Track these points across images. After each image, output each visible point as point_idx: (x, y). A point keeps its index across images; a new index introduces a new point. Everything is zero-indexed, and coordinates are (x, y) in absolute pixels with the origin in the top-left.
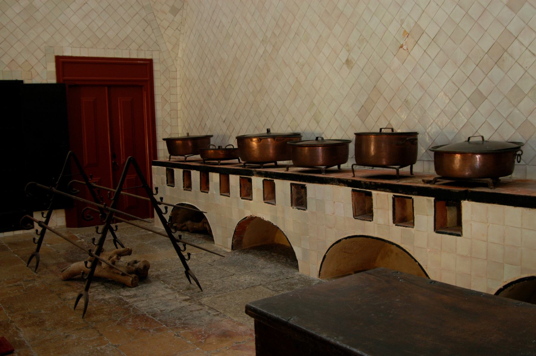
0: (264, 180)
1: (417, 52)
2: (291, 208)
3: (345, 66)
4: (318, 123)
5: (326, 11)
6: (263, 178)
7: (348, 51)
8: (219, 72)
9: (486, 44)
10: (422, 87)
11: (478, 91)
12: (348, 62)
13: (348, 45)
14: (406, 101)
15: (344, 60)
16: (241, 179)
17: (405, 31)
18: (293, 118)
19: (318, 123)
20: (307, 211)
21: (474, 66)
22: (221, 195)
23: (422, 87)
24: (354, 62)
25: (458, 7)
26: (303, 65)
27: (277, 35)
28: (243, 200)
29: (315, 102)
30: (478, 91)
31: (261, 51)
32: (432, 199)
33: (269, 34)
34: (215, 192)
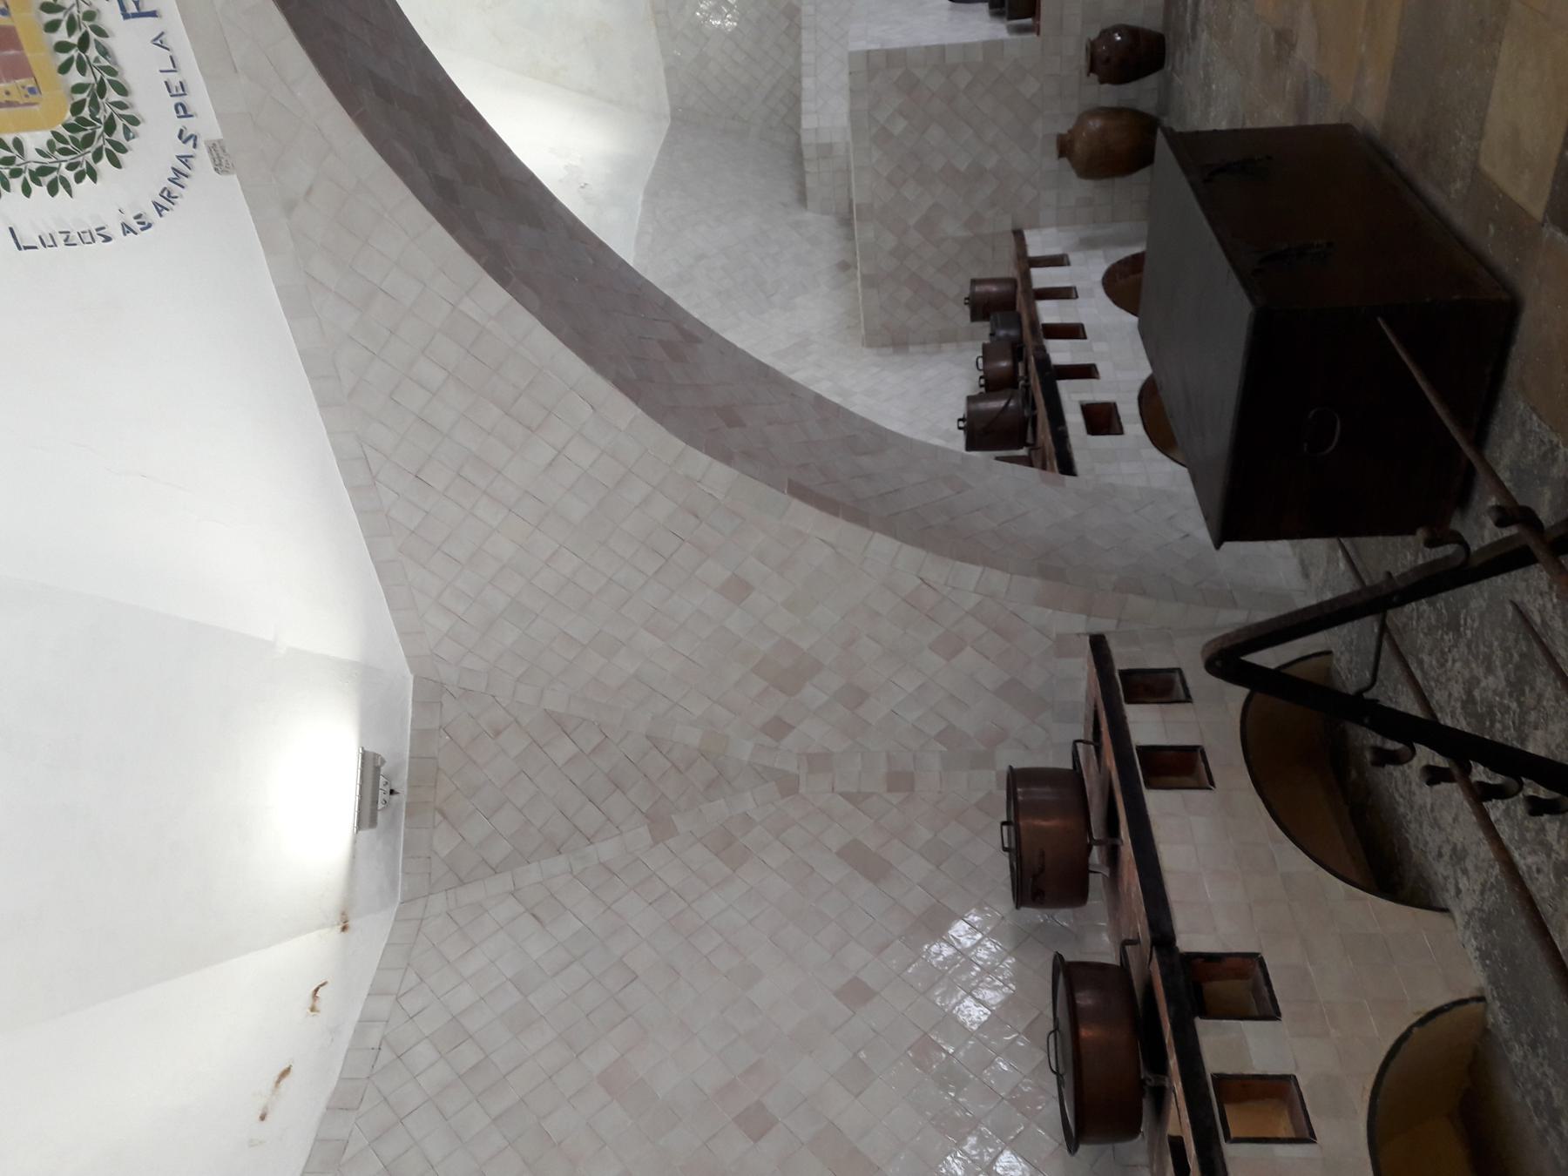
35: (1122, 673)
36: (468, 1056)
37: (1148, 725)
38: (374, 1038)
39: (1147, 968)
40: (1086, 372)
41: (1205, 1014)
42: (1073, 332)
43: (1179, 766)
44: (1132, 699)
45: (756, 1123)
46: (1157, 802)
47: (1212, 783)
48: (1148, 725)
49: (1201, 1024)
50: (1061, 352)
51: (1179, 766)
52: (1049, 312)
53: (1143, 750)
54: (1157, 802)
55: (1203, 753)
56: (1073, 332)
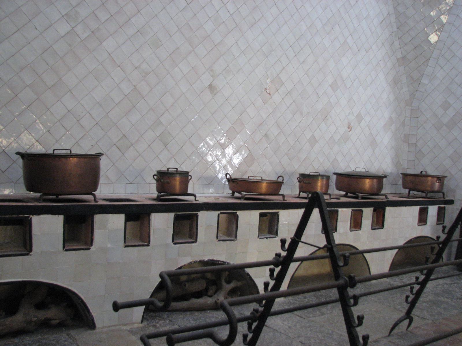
0: (221, 213)
1: (277, 98)
4: (166, 145)
7: (212, 76)
11: (313, 136)
12: (211, 87)
13: (212, 71)
14: (266, 135)
15: (207, 84)
16: (177, 219)
18: (124, 136)
19: (166, 145)
21: (312, 119)
22: (126, 246)
24: (218, 90)
25: (306, 75)
29: (162, 119)
31: (63, 28)
32: (372, 209)
37: (433, 210)
39: (382, 198)
41: (374, 210)
43: (423, 219)
44: (439, 208)
45: (334, 87)
46: (416, 209)
47: (419, 225)
48: (433, 210)
49: (372, 209)
53: (427, 208)
54: (416, 209)
55: (425, 225)
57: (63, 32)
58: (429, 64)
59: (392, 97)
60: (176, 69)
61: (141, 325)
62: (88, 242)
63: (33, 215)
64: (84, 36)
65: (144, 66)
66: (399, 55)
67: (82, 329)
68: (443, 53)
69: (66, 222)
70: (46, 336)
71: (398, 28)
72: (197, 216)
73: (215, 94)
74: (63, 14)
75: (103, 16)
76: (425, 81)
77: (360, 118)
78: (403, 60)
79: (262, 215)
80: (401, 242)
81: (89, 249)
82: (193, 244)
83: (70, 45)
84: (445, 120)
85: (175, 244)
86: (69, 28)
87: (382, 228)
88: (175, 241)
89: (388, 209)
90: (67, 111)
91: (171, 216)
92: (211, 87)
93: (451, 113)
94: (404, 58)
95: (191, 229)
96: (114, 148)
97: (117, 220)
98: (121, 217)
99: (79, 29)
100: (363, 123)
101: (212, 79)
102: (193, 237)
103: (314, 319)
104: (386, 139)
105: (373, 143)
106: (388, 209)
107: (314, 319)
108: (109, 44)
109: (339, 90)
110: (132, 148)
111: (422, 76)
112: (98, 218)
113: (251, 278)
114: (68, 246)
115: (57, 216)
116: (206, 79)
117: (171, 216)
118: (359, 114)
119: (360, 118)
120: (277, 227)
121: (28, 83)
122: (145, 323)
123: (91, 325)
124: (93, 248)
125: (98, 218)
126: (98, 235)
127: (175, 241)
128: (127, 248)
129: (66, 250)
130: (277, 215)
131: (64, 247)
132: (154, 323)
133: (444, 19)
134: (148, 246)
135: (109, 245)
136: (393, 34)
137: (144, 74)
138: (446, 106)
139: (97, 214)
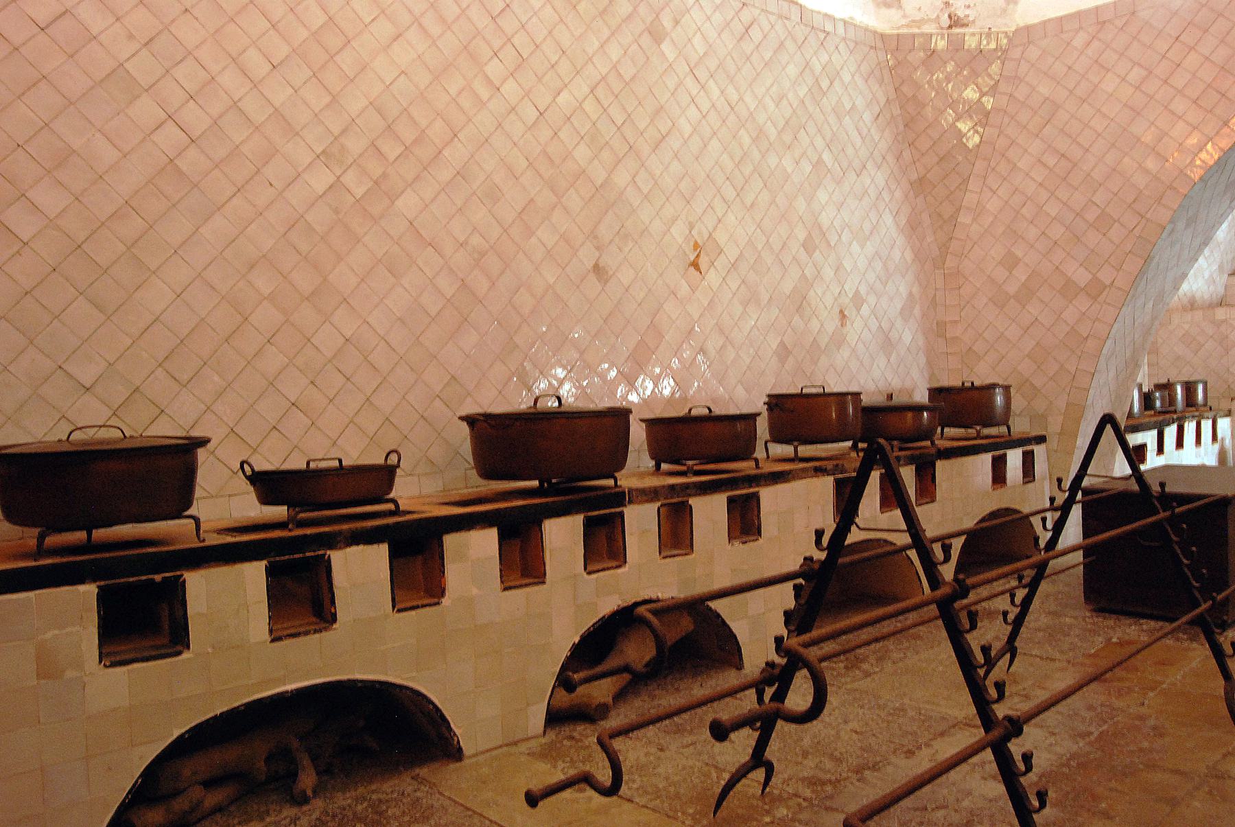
1: (713, 278)
2: (729, 547)
3: (592, 277)
5: (544, 152)
6: (659, 504)
7: (598, 248)
8: (49, 199)
9: (787, 287)
10: (721, 331)
12: (597, 269)
13: (596, 237)
15: (589, 264)
16: (589, 525)
17: (696, 243)
20: (761, 541)
22: (505, 589)
23: (721, 331)
24: (611, 273)
26: (483, 254)
27: (392, 158)
28: (594, 576)
30: (782, 343)
31: (320, 180)
33: (355, 145)
34: (475, 591)
35: (1032, 452)
36: (825, 84)
37: (1014, 458)
38: (829, 28)
40: (1160, 450)
42: (1180, 444)
43: (999, 477)
44: (1024, 453)
46: (987, 458)
48: (1014, 458)
49: (914, 467)
50: (1171, 432)
51: (999, 477)
52: (1190, 428)
53: (1005, 455)
56: (1180, 444)
57: (320, 187)
58: (970, 187)
59: (909, 256)
60: (533, 240)
61: (543, 740)
62: (434, 590)
63: (331, 548)
64: (359, 192)
65: (476, 240)
66: (914, 176)
67: (437, 765)
68: (993, 164)
69: (393, 556)
70: (374, 787)
71: (906, 126)
72: (621, 515)
73: (606, 282)
74: (319, 150)
75: (392, 150)
76: (964, 219)
77: (858, 300)
78: (920, 186)
79: (731, 501)
80: (969, 523)
81: (438, 604)
82: (620, 571)
83: (336, 211)
84: (1012, 289)
85: (589, 573)
86: (332, 179)
87: (933, 501)
88: (590, 568)
89: (939, 464)
90: (343, 340)
91: (575, 523)
92: (597, 269)
93: (1021, 274)
94: (921, 180)
95: (611, 539)
96: (438, 403)
97: (485, 542)
98: (493, 534)
99: (350, 179)
100: (865, 310)
101: (597, 254)
102: (617, 555)
103: (855, 685)
104: (908, 335)
105: (887, 344)
106: (939, 464)
107: (855, 685)
108: (408, 203)
109: (817, 252)
110: (469, 400)
111: (958, 210)
112: (451, 541)
113: (723, 622)
114: (402, 602)
115: (375, 546)
116: (587, 256)
117: (575, 523)
118: (857, 292)
119: (858, 300)
120: (759, 518)
121: (266, 291)
122: (551, 735)
123: (453, 752)
124: (445, 601)
125: (451, 541)
126: (454, 575)
127: (590, 568)
128: (506, 593)
129: (399, 611)
130: (755, 497)
131: (394, 607)
132: (568, 733)
133: (988, 102)
134: (544, 583)
135: (475, 591)
136: (900, 138)
137: (476, 256)
138: (1011, 262)
139: (448, 532)
